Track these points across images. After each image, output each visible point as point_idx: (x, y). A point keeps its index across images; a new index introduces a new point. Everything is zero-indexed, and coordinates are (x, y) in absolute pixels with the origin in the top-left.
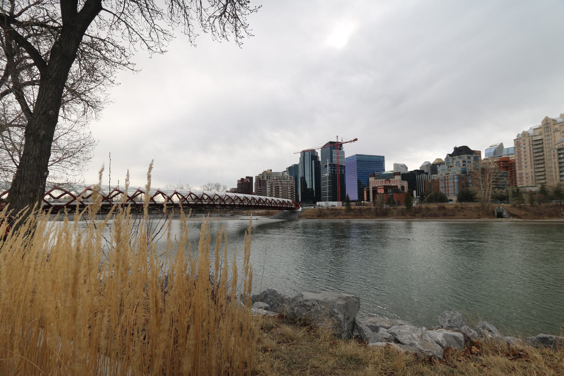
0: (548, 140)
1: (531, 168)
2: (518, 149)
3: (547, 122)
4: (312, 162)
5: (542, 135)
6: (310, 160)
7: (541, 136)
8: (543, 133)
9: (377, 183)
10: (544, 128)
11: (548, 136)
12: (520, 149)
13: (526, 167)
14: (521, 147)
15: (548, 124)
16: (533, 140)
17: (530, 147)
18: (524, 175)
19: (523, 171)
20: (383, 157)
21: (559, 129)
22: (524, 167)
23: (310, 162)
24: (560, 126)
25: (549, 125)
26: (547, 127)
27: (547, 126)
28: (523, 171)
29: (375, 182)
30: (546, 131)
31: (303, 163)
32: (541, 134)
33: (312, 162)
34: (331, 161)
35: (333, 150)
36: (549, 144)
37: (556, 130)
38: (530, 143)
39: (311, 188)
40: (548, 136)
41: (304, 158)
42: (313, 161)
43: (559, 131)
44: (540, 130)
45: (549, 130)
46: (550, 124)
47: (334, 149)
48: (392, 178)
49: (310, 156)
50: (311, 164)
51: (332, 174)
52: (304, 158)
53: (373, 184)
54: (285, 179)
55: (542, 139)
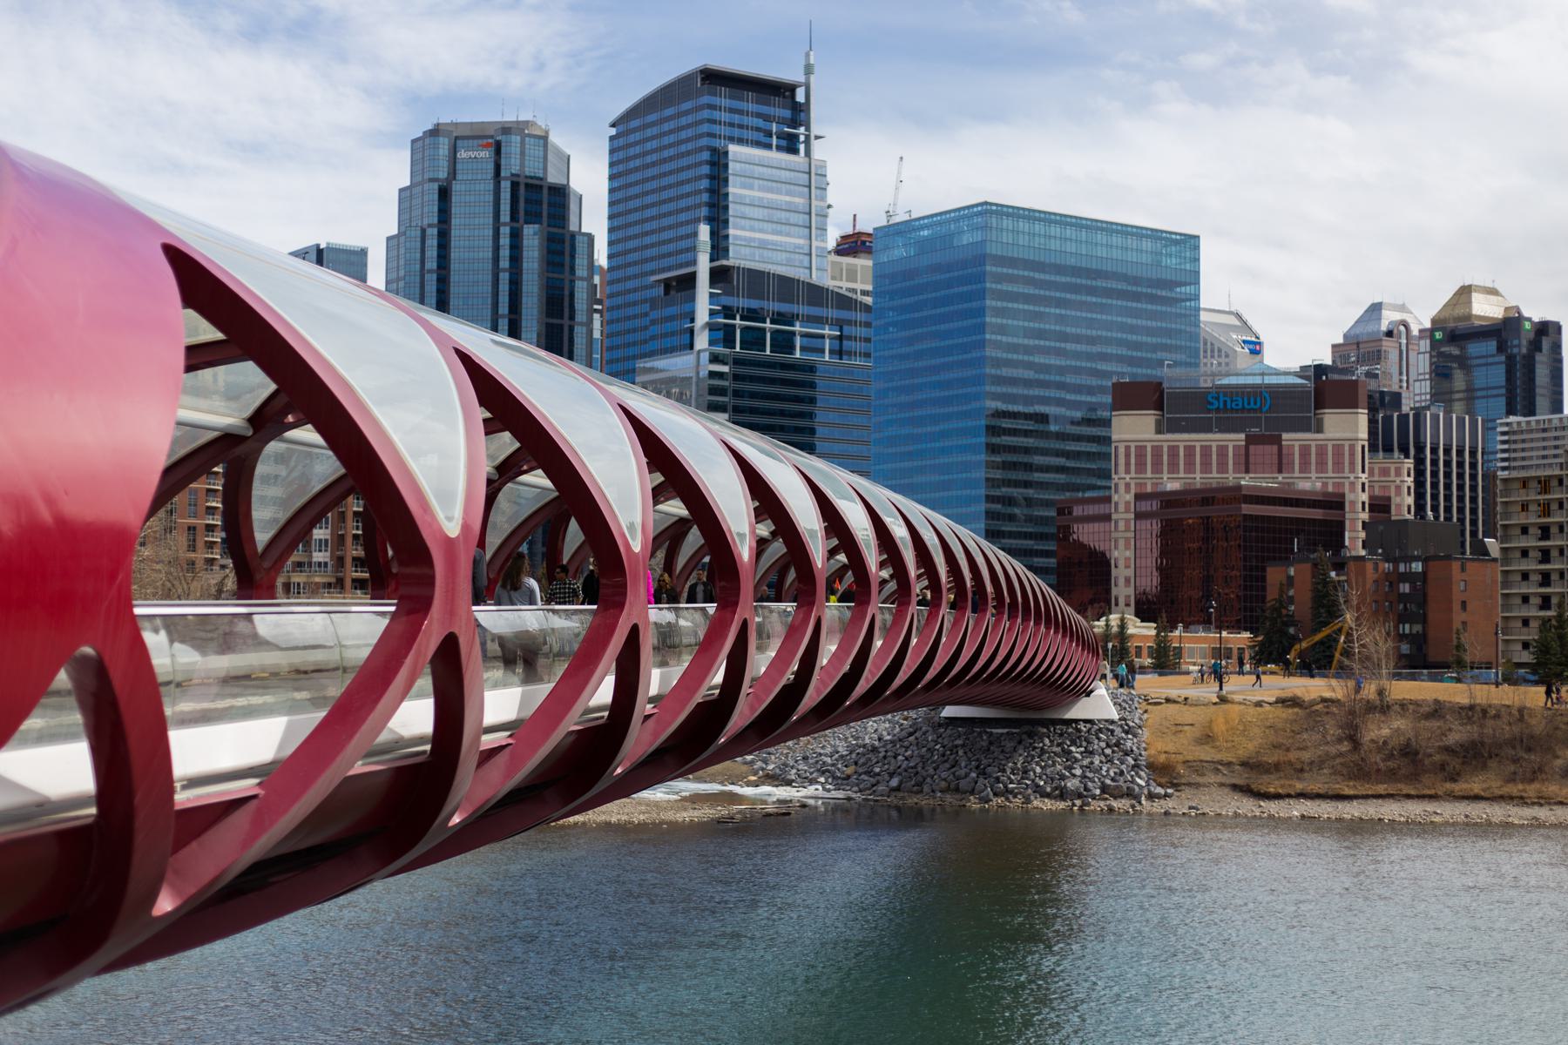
4: (516, 236)
6: (505, 216)
9: (1173, 467)
20: (1189, 244)
23: (505, 241)
29: (1157, 452)
31: (432, 243)
33: (516, 236)
34: (719, 246)
35: (733, 149)
41: (444, 194)
42: (532, 236)
47: (741, 141)
48: (1304, 426)
49: (506, 186)
50: (505, 253)
51: (737, 362)
52: (444, 194)
53: (1141, 466)
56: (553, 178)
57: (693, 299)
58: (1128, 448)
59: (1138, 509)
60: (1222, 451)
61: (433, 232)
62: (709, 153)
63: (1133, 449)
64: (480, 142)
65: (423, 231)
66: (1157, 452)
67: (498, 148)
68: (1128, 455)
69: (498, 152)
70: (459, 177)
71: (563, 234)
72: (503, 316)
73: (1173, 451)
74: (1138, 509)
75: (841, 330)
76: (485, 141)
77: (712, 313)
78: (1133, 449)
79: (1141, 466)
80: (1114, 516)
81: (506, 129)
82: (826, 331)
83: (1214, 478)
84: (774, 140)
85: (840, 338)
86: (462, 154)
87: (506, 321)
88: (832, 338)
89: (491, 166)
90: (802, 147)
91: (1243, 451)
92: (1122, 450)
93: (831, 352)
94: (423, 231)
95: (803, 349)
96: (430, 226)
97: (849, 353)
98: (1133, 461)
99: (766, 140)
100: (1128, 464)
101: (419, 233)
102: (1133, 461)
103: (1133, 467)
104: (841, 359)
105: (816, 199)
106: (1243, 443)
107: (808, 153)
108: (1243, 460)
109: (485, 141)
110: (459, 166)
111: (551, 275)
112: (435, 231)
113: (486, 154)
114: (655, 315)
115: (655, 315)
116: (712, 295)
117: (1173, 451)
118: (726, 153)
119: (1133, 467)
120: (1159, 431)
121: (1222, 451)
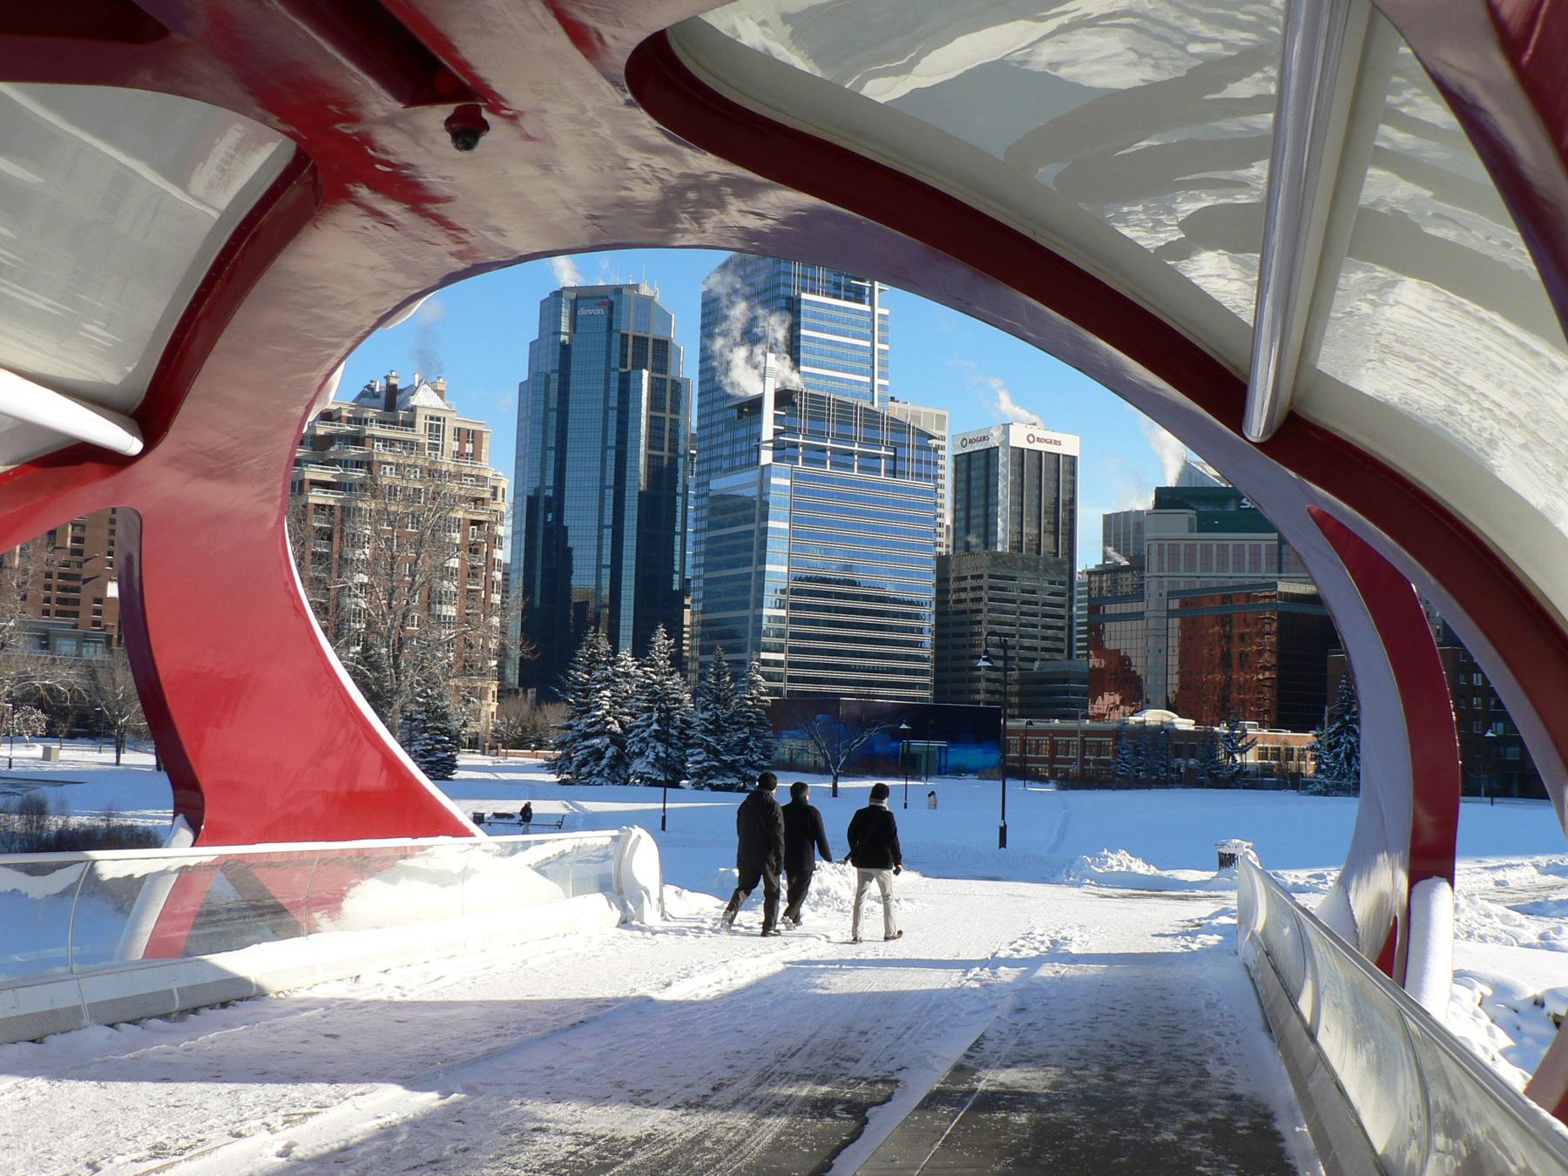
6: (615, 364)
23: (614, 384)
29: (1191, 550)
31: (554, 386)
35: (804, 296)
39: (606, 592)
49: (616, 337)
53: (1174, 565)
54: (410, 445)
56: (654, 333)
57: (760, 422)
58: (1161, 547)
59: (1170, 608)
60: (1255, 552)
61: (556, 376)
62: (784, 301)
63: (1166, 548)
64: (597, 301)
65: (548, 376)
66: (1191, 550)
67: (611, 307)
68: (1161, 554)
69: (611, 309)
70: (578, 330)
71: (665, 380)
72: (611, 448)
73: (1207, 550)
74: (1170, 608)
75: (895, 451)
76: (600, 301)
77: (777, 433)
78: (1166, 548)
79: (1174, 565)
80: (1146, 614)
81: (618, 290)
82: (883, 452)
83: (1247, 576)
84: (843, 293)
85: (894, 458)
86: (582, 312)
87: (613, 452)
88: (886, 457)
89: (605, 321)
90: (867, 299)
91: (1276, 550)
92: (1154, 548)
93: (886, 471)
94: (548, 376)
95: (860, 468)
96: (553, 371)
97: (902, 473)
98: (1166, 559)
99: (837, 292)
100: (1161, 563)
101: (543, 379)
102: (1166, 559)
103: (1166, 566)
104: (895, 477)
105: (879, 342)
106: (1276, 543)
107: (872, 304)
108: (1275, 559)
109: (600, 301)
110: (579, 322)
111: (654, 414)
112: (557, 376)
113: (601, 311)
114: (727, 437)
115: (727, 437)
116: (776, 416)
117: (1207, 550)
118: (799, 300)
119: (1166, 566)
120: (1191, 531)
121: (1255, 552)
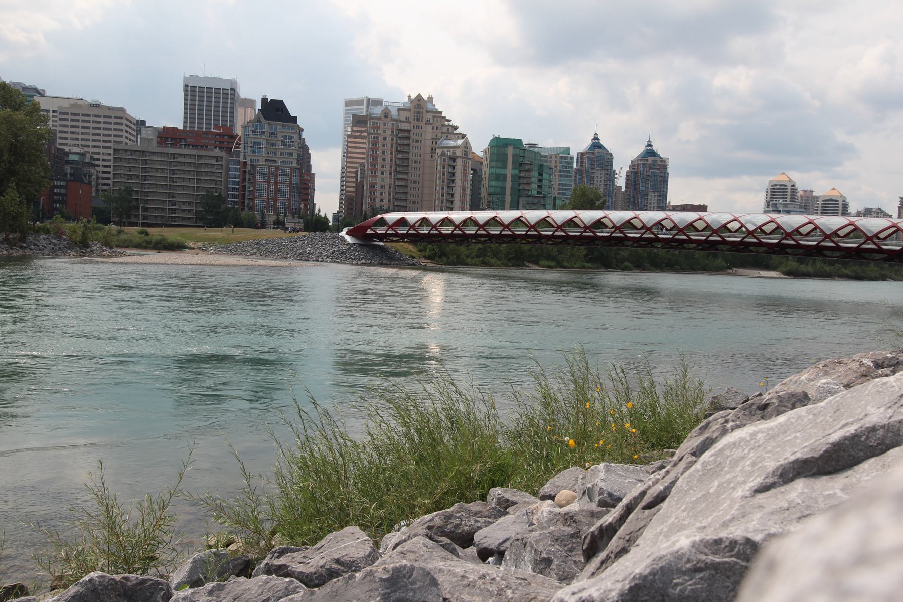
0: (417, 135)
1: (390, 178)
2: (374, 138)
3: (419, 103)
5: (410, 123)
7: (408, 125)
8: (412, 120)
10: (415, 112)
11: (418, 127)
12: (377, 138)
13: (383, 173)
14: (379, 134)
15: (420, 108)
16: (400, 128)
17: (392, 139)
18: (378, 187)
19: (378, 180)
21: (431, 122)
22: (379, 173)
24: (434, 117)
25: (421, 111)
26: (418, 113)
27: (419, 110)
28: (378, 180)
30: (416, 118)
32: (407, 121)
36: (417, 141)
37: (428, 122)
38: (393, 132)
40: (418, 127)
43: (431, 124)
44: (407, 114)
45: (421, 118)
46: (423, 108)
55: (409, 131)
